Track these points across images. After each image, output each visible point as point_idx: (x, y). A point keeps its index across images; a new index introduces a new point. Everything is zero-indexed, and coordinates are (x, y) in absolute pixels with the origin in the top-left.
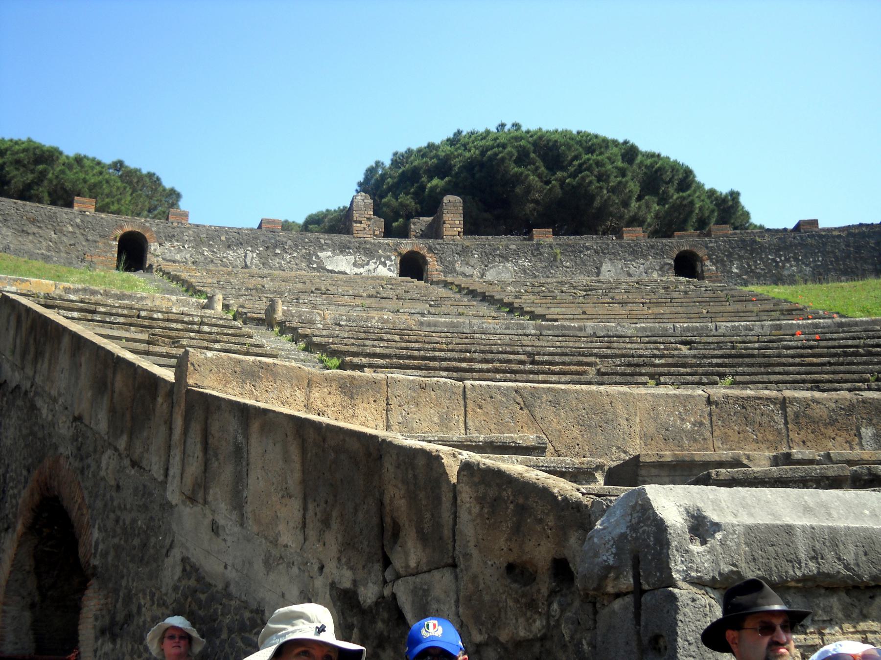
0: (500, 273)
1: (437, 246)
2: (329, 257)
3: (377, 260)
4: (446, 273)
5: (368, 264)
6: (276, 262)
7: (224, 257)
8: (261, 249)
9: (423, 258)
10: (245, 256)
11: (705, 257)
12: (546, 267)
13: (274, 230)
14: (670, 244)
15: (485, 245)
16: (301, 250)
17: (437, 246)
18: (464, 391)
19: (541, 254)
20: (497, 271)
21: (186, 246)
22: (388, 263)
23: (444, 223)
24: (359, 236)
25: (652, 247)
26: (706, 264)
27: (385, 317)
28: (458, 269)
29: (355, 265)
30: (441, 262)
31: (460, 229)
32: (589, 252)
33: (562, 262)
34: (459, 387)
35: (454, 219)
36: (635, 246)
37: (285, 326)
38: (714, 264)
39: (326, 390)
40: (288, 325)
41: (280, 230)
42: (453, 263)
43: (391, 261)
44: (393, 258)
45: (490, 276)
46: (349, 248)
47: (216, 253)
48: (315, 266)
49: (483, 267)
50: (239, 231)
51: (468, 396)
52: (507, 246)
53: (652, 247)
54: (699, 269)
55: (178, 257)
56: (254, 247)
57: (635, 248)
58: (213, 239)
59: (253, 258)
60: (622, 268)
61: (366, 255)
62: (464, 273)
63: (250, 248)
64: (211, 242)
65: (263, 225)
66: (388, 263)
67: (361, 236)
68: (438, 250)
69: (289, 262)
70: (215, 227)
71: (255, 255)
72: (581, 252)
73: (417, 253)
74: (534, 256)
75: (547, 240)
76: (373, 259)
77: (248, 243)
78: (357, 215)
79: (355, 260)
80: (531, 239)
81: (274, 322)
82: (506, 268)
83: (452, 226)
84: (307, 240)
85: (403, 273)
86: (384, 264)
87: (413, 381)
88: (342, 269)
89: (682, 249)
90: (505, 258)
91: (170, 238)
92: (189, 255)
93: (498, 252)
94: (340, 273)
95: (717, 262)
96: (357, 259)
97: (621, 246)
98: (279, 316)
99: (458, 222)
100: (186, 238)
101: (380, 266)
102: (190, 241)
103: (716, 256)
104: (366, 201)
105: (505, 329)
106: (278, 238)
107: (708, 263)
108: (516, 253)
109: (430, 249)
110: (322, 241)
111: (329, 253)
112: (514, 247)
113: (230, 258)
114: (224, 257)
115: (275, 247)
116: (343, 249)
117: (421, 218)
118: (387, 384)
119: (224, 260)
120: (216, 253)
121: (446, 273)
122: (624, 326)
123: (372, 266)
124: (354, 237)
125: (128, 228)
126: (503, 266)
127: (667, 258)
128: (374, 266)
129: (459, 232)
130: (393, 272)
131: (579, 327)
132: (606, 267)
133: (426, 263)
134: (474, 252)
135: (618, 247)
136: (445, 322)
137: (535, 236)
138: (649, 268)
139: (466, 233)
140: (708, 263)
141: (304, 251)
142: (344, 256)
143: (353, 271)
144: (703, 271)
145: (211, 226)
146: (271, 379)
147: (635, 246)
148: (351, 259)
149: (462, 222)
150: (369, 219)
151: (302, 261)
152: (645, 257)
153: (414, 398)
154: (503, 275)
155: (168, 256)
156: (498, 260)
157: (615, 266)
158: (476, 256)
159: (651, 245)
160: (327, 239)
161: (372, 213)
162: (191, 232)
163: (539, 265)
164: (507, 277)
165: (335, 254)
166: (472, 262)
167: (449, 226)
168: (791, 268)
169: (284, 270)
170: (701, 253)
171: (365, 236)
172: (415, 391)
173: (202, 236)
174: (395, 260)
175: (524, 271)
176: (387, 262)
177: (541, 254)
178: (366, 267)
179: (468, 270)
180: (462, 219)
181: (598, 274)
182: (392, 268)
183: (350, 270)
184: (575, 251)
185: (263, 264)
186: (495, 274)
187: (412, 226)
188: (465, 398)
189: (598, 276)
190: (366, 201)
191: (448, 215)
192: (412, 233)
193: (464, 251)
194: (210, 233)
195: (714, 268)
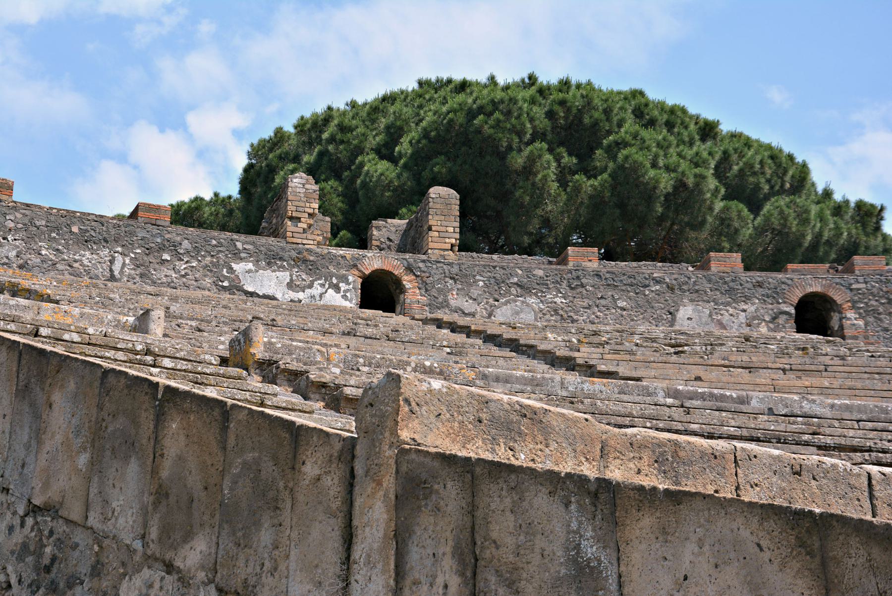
0: (517, 313)
1: (421, 265)
2: (249, 271)
3: (326, 280)
4: (432, 307)
5: (310, 286)
6: (163, 274)
7: (76, 261)
8: (138, 251)
9: (398, 282)
10: (112, 262)
11: (847, 306)
12: (589, 307)
13: (159, 223)
14: (789, 282)
15: (494, 267)
16: (204, 256)
17: (421, 265)
18: (870, 485)
19: (582, 286)
20: (512, 309)
21: (10, 238)
22: (343, 286)
23: (430, 229)
24: (294, 240)
25: (760, 285)
26: (849, 315)
27: (428, 363)
28: (453, 303)
29: (291, 286)
30: (427, 290)
31: (453, 241)
32: (658, 287)
33: (615, 300)
34: (859, 475)
35: (444, 223)
36: (733, 281)
37: (278, 368)
38: (861, 317)
39: (631, 465)
40: (282, 367)
41: (168, 224)
42: (444, 292)
43: (348, 283)
44: (351, 278)
46: (281, 259)
47: (63, 253)
48: (226, 284)
49: (491, 301)
50: (100, 220)
51: (877, 494)
52: (529, 270)
53: (760, 285)
54: (835, 324)
56: (127, 248)
57: (731, 284)
58: (57, 229)
59: (124, 265)
60: (710, 315)
61: (309, 272)
62: (461, 310)
63: (119, 249)
64: (54, 235)
65: (140, 213)
66: (343, 286)
67: (299, 241)
68: (421, 271)
69: (183, 276)
70: (59, 210)
71: (127, 261)
72: (646, 286)
73: (388, 273)
74: (572, 289)
75: (589, 264)
76: (319, 279)
78: (294, 208)
79: (291, 280)
80: (564, 261)
81: (251, 362)
82: (528, 305)
83: (442, 234)
84: (214, 242)
85: (365, 303)
86: (337, 288)
87: (778, 458)
88: (269, 292)
89: (810, 290)
90: (524, 288)
92: (14, 253)
93: (515, 280)
94: (265, 297)
95: (867, 313)
96: (294, 278)
97: (710, 281)
98: (258, 351)
99: (451, 230)
100: (11, 225)
101: (331, 291)
102: (17, 230)
103: (866, 304)
104: (307, 186)
105: (619, 393)
106: (167, 236)
107: (851, 314)
108: (542, 283)
109: (409, 269)
110: (239, 245)
111: (250, 266)
112: (540, 273)
113: (86, 262)
114: (76, 261)
115: (162, 248)
116: (272, 260)
117: (389, 220)
118: (736, 462)
119: (76, 265)
120: (63, 253)
121: (432, 307)
122: (814, 401)
123: (317, 290)
124: (287, 243)
126: (523, 302)
127: (785, 302)
128: (320, 290)
129: (452, 245)
130: (351, 301)
131: (738, 397)
132: (685, 312)
133: (401, 289)
134: (478, 277)
135: (704, 281)
136: (523, 376)
137: (570, 258)
138: (754, 318)
139: (464, 247)
140: (851, 314)
141: (209, 259)
142: (274, 271)
143: (286, 296)
144: (841, 327)
145: (51, 208)
146: (540, 438)
147: (733, 281)
148: (285, 276)
149: (458, 230)
150: (311, 215)
151: (205, 276)
152: (747, 299)
153: (783, 489)
154: (522, 315)
156: (515, 292)
157: (699, 312)
158: (481, 283)
159: (758, 282)
160: (247, 243)
161: (317, 206)
162: (19, 215)
163: (579, 302)
164: (528, 317)
165: (258, 268)
166: (475, 292)
167: (436, 234)
169: (176, 288)
170: (838, 297)
171: (305, 242)
172: (782, 476)
173: (38, 223)
174: (354, 279)
175: (556, 311)
176: (341, 285)
177: (582, 286)
178: (308, 291)
179: (468, 305)
180: (457, 224)
181: (672, 323)
182: (348, 294)
183: (284, 295)
184: (638, 286)
185: (142, 276)
186: (509, 313)
187: (375, 232)
188: (871, 496)
189: (672, 326)
190: (307, 186)
191: (437, 218)
192: (374, 243)
193: (462, 278)
194: (52, 218)
195: (861, 323)
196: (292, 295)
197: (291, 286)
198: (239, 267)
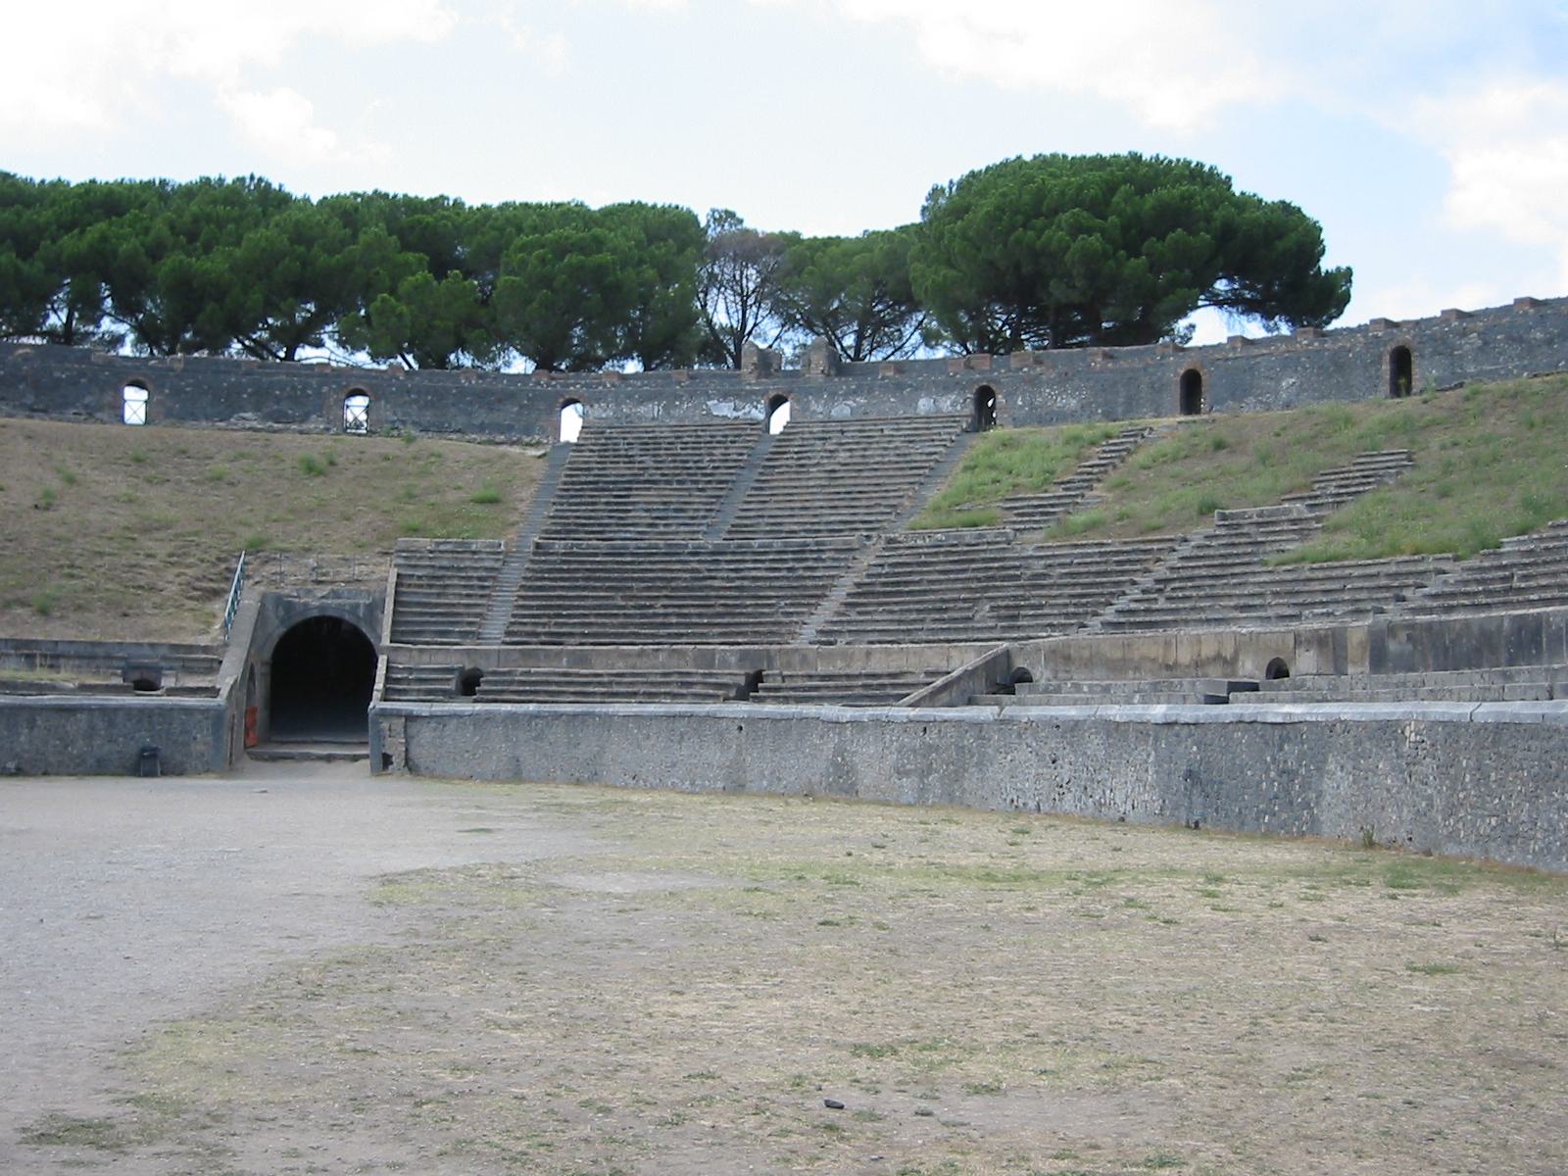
6: (676, 412)
29: (735, 409)
42: (808, 402)
55: (604, 416)
77: (655, 398)
90: (846, 396)
91: (598, 401)
95: (1007, 396)
123: (747, 410)
125: (567, 397)
155: (596, 414)
164: (847, 411)
179: (820, 409)
181: (916, 408)
196: (735, 414)
197: (735, 409)
198: (709, 403)
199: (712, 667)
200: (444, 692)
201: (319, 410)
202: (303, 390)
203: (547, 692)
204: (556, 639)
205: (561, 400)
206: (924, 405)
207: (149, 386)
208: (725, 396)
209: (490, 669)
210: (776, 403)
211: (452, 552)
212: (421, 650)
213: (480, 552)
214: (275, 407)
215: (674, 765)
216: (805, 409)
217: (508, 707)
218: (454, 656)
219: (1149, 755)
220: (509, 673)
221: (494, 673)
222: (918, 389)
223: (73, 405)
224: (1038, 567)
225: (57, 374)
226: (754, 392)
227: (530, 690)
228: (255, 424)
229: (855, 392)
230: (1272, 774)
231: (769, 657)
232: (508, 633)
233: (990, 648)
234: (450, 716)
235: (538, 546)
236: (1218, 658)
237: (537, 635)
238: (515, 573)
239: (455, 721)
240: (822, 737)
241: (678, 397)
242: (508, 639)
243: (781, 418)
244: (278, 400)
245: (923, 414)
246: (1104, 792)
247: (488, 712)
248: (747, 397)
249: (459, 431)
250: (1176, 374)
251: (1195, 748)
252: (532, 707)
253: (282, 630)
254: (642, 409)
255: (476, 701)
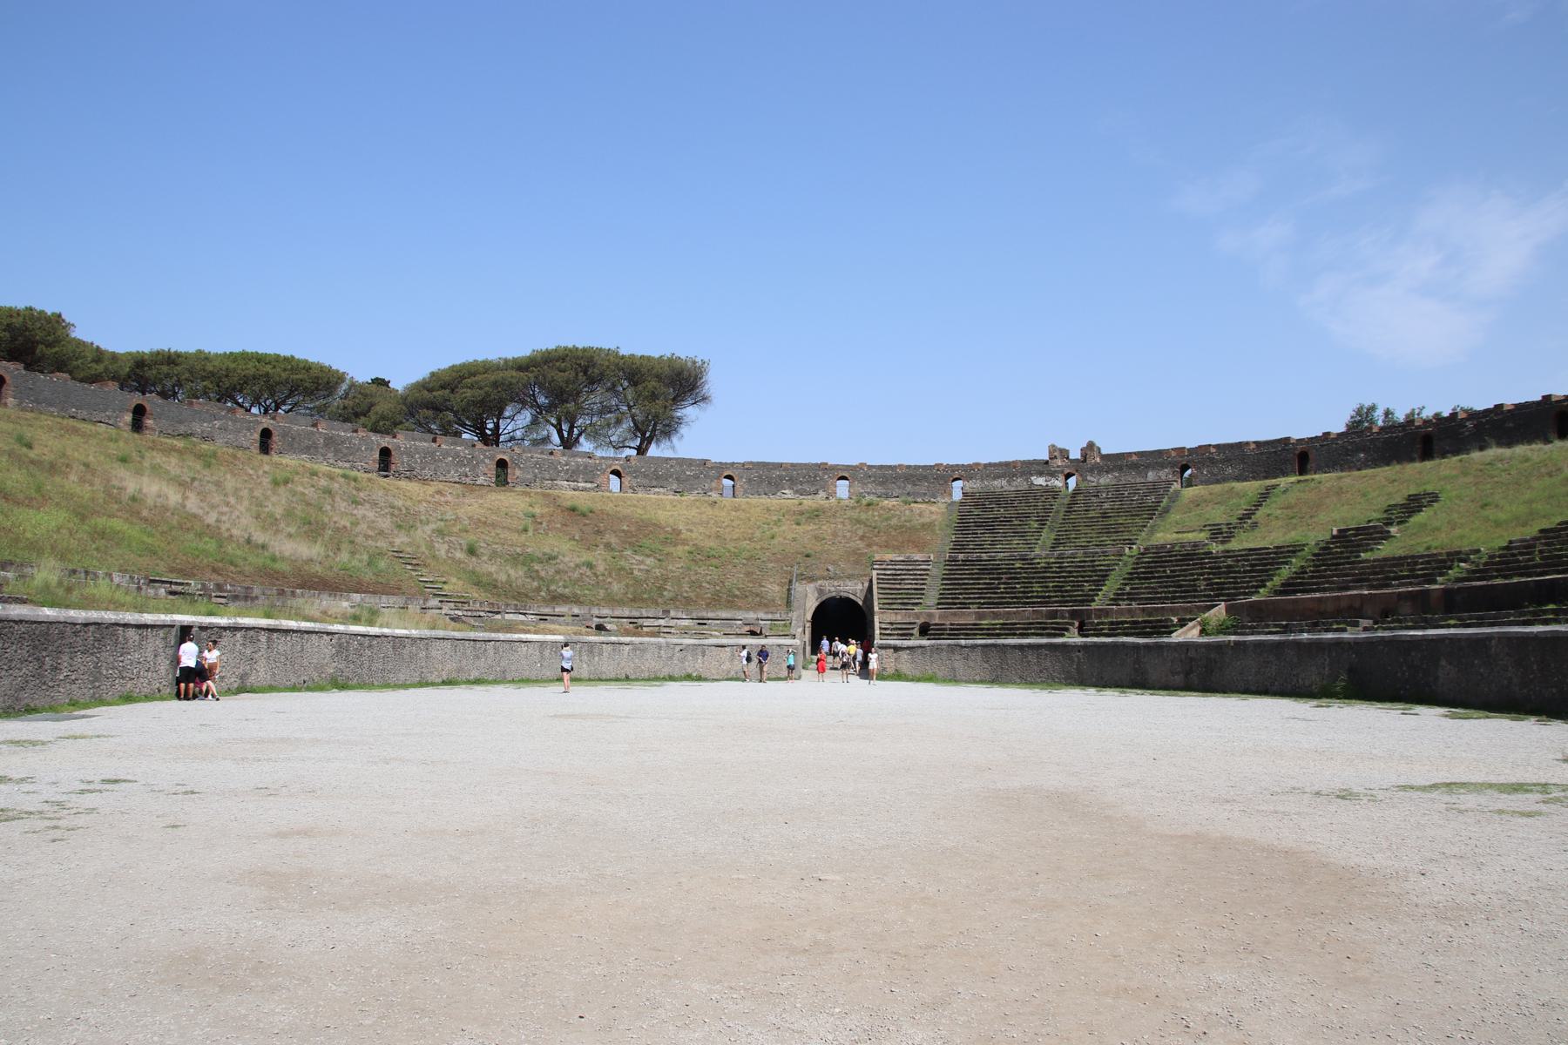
29: (1046, 481)
45: (1102, 481)
90: (1107, 472)
91: (971, 479)
123: (1053, 481)
125: (955, 477)
132: (1150, 474)
152: (1166, 468)
168: (1229, 470)
179: (1092, 479)
183: (1044, 484)
197: (1046, 481)
198: (1032, 478)
199: (1056, 618)
200: (912, 635)
201: (824, 488)
202: (815, 476)
203: (967, 634)
204: (965, 605)
205: (951, 479)
206: (1151, 476)
207: (736, 479)
208: (1040, 474)
209: (934, 622)
210: (1068, 476)
211: (903, 561)
212: (896, 613)
213: (917, 561)
214: (800, 487)
215: (1041, 672)
216: (1085, 480)
217: (949, 641)
218: (919, 615)
219: (1325, 660)
220: (943, 624)
221: (936, 624)
222: (1148, 467)
223: (696, 489)
224: (1229, 561)
225: (688, 473)
226: (1056, 471)
227: (957, 632)
228: (790, 496)
229: (1112, 470)
230: (1404, 668)
231: (1089, 613)
232: (939, 604)
233: (1217, 605)
234: (917, 647)
235: (949, 556)
236: (1350, 607)
237: (955, 604)
238: (936, 571)
239: (920, 650)
240: (1127, 655)
241: (1015, 475)
242: (940, 607)
243: (1072, 482)
244: (802, 484)
245: (1150, 480)
246: (1298, 681)
247: (938, 645)
248: (1053, 474)
249: (898, 497)
250: (1294, 454)
251: (1354, 656)
252: (963, 642)
253: (818, 603)
254: (996, 483)
255: (929, 639)
